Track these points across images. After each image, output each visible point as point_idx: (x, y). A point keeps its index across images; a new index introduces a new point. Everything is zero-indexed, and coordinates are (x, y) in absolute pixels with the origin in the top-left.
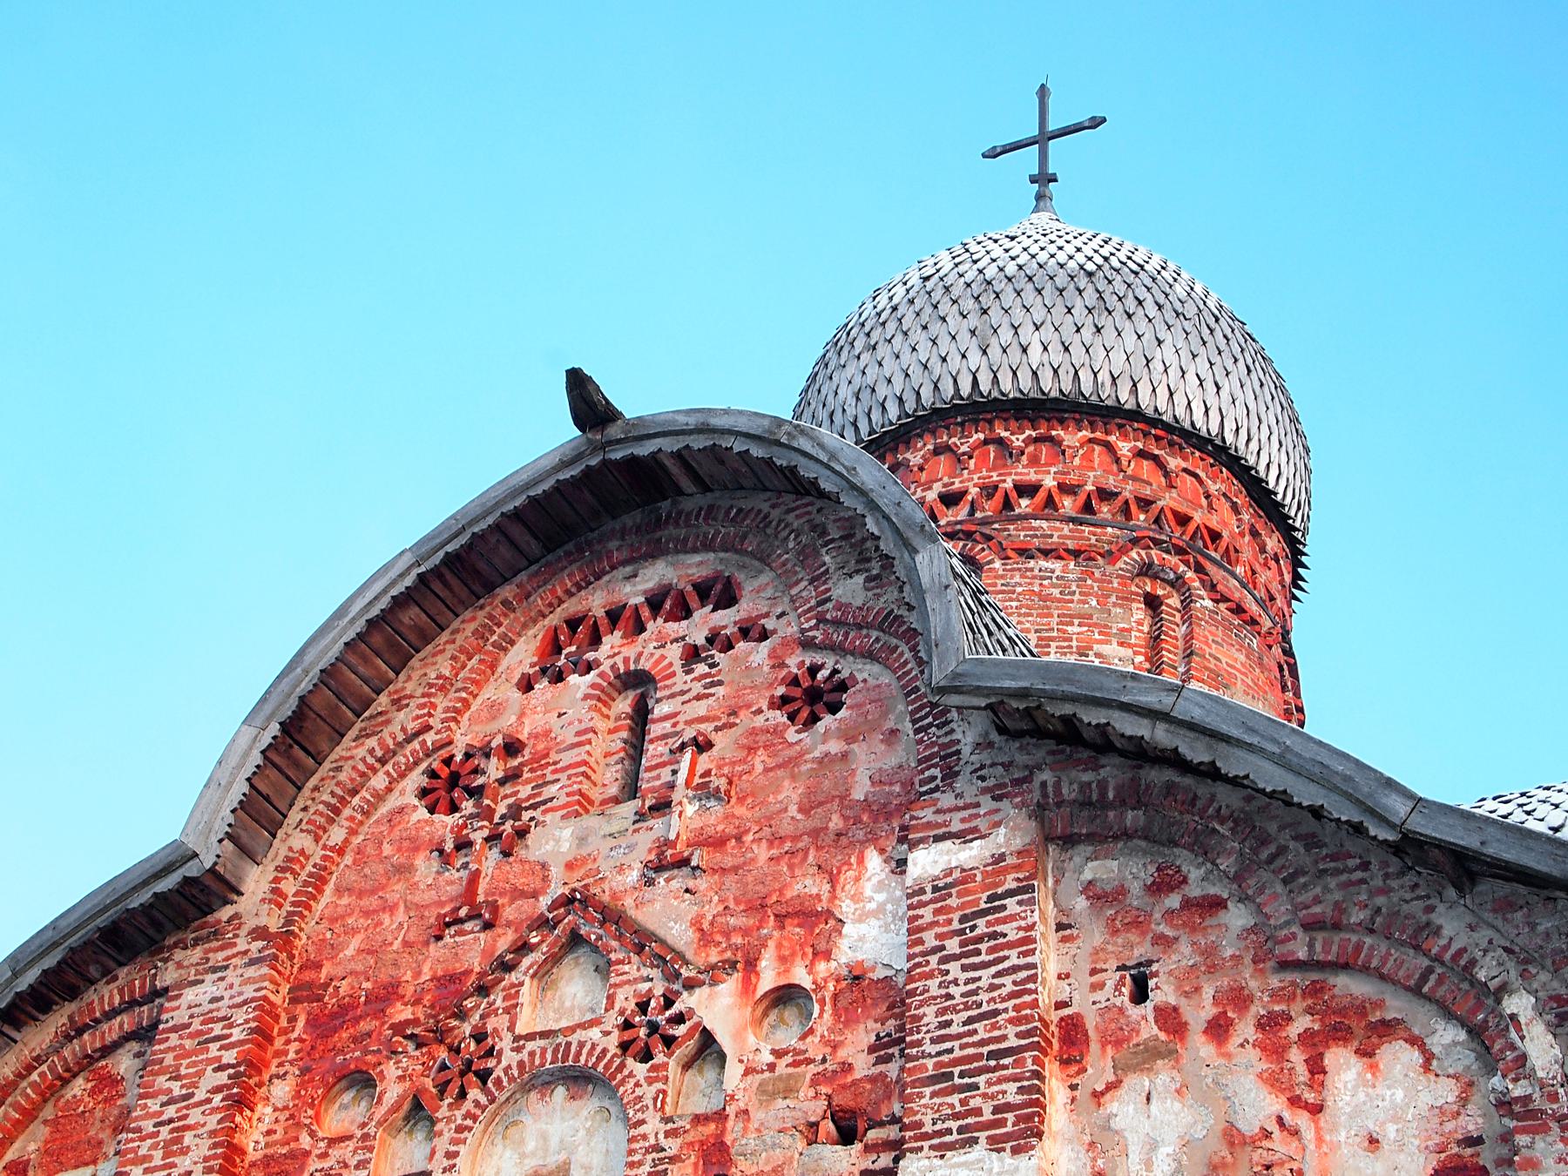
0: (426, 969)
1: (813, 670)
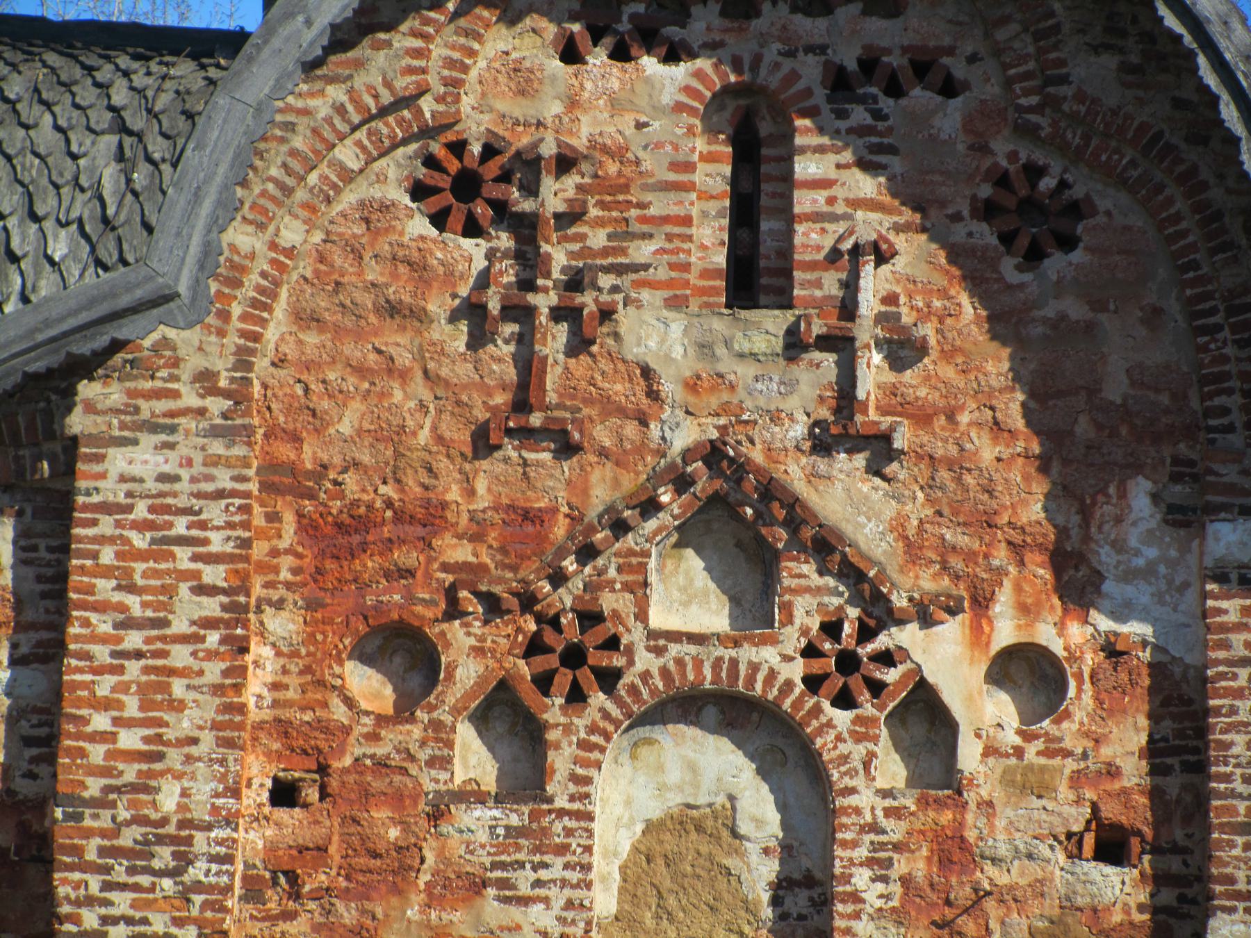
0: (481, 486)
1: (1034, 172)
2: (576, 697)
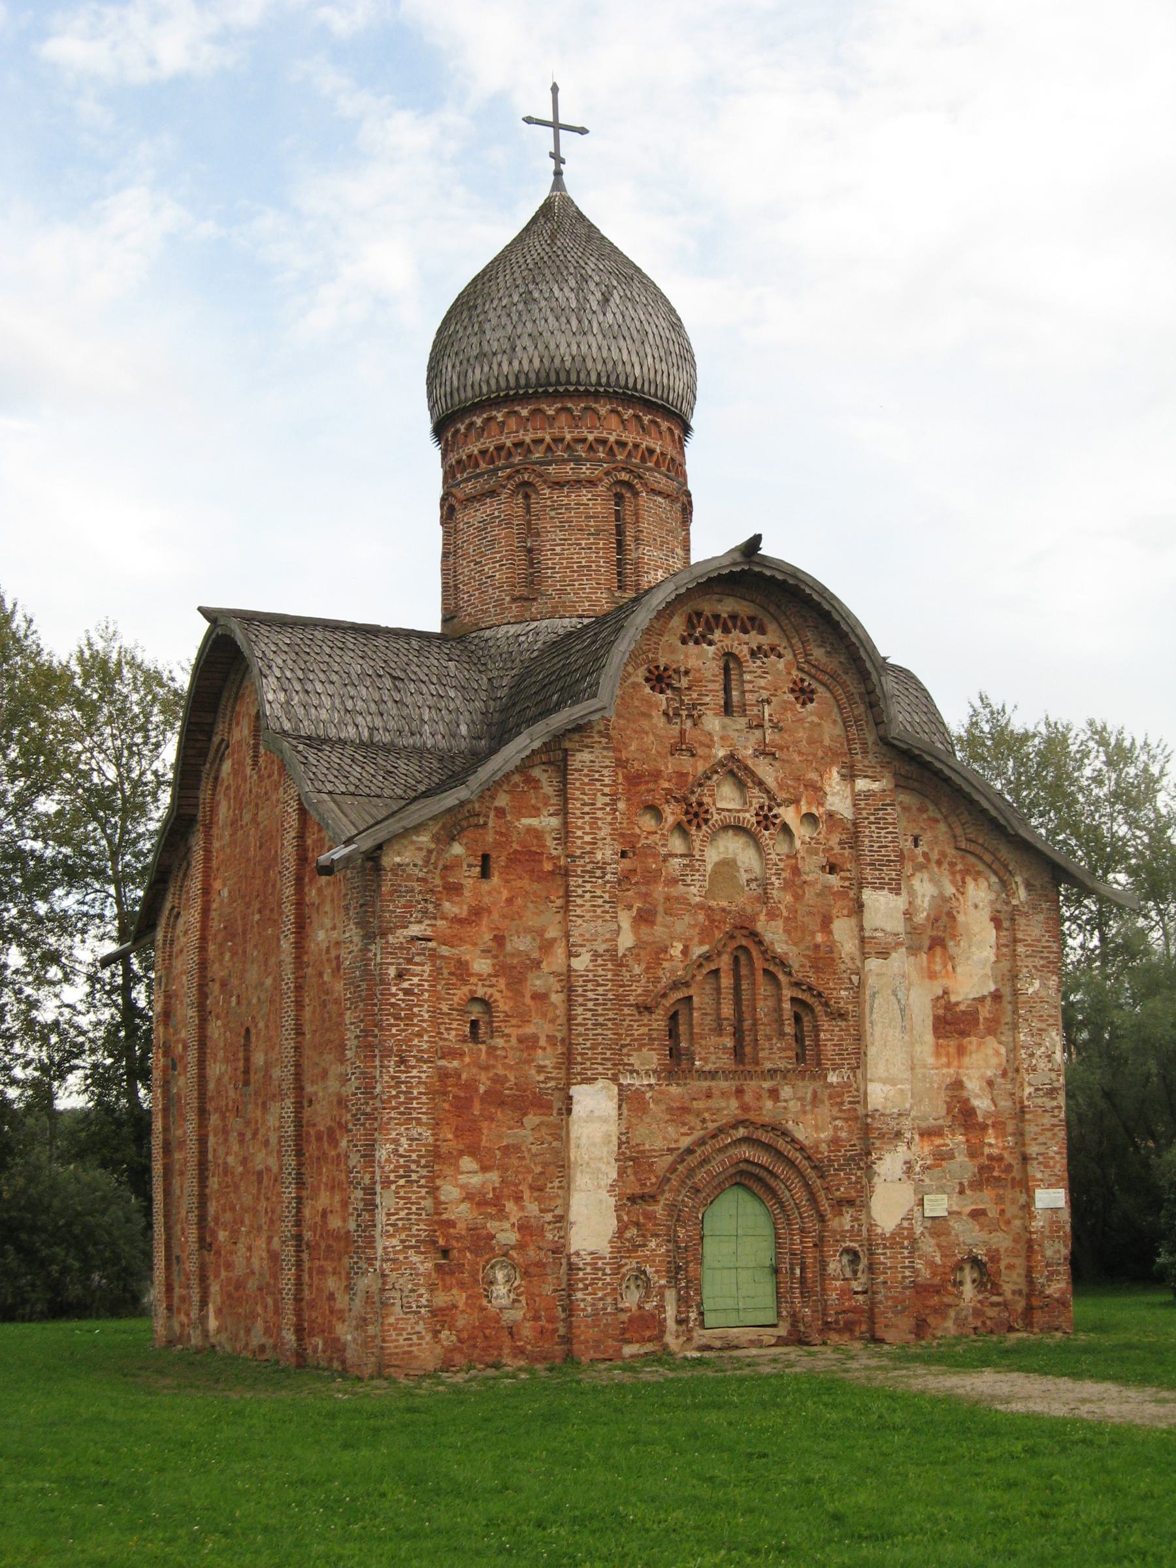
1: (802, 680)
2: (699, 827)
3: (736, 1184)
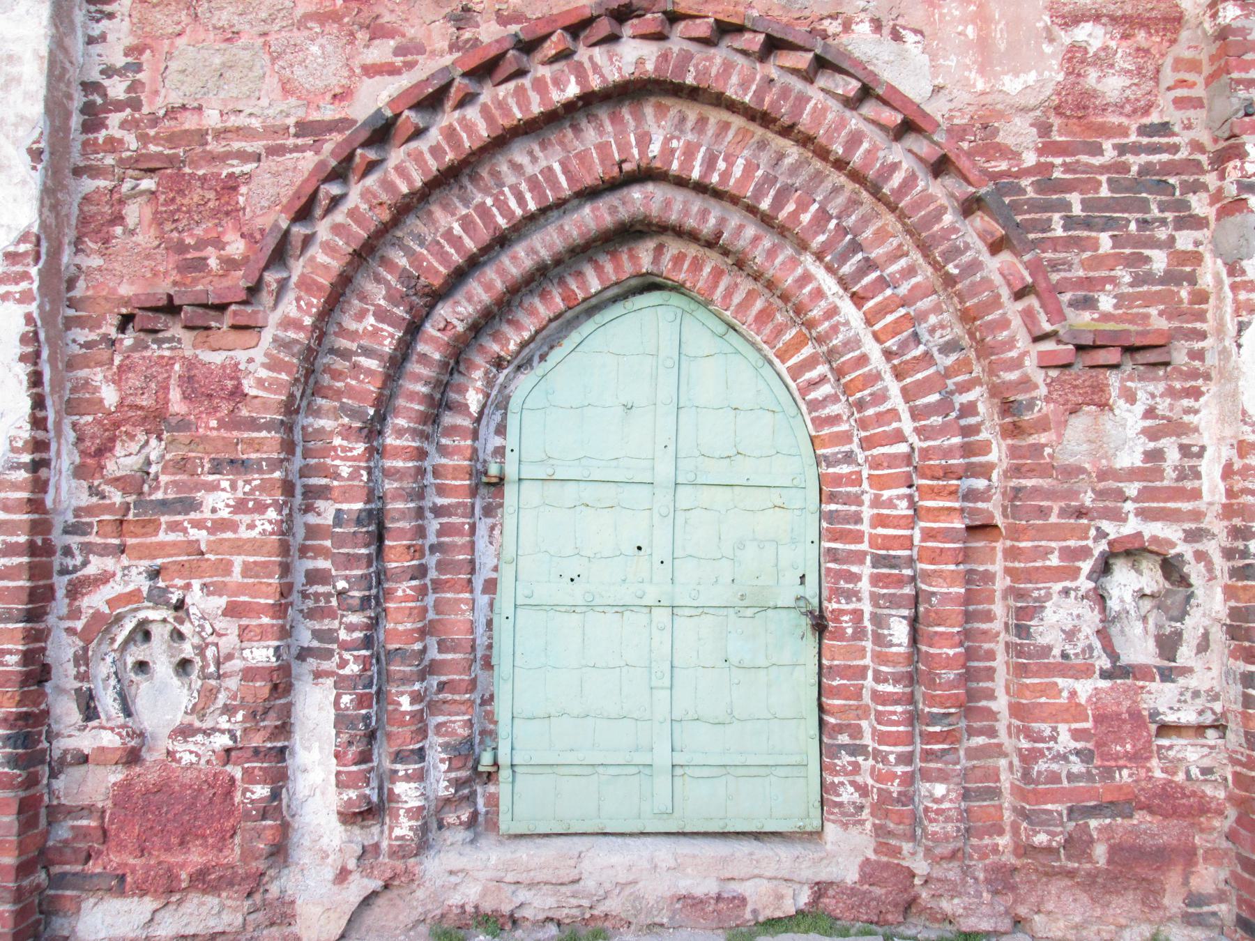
3: (649, 284)
